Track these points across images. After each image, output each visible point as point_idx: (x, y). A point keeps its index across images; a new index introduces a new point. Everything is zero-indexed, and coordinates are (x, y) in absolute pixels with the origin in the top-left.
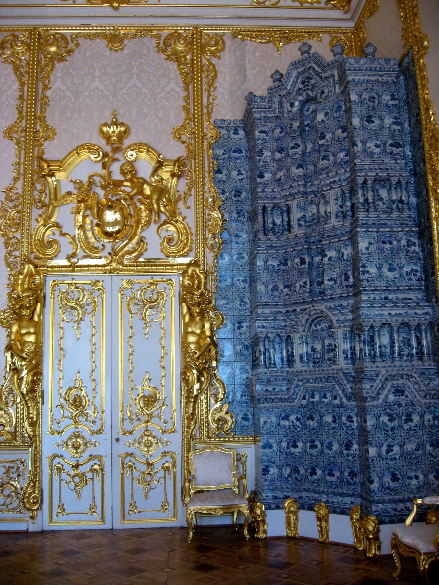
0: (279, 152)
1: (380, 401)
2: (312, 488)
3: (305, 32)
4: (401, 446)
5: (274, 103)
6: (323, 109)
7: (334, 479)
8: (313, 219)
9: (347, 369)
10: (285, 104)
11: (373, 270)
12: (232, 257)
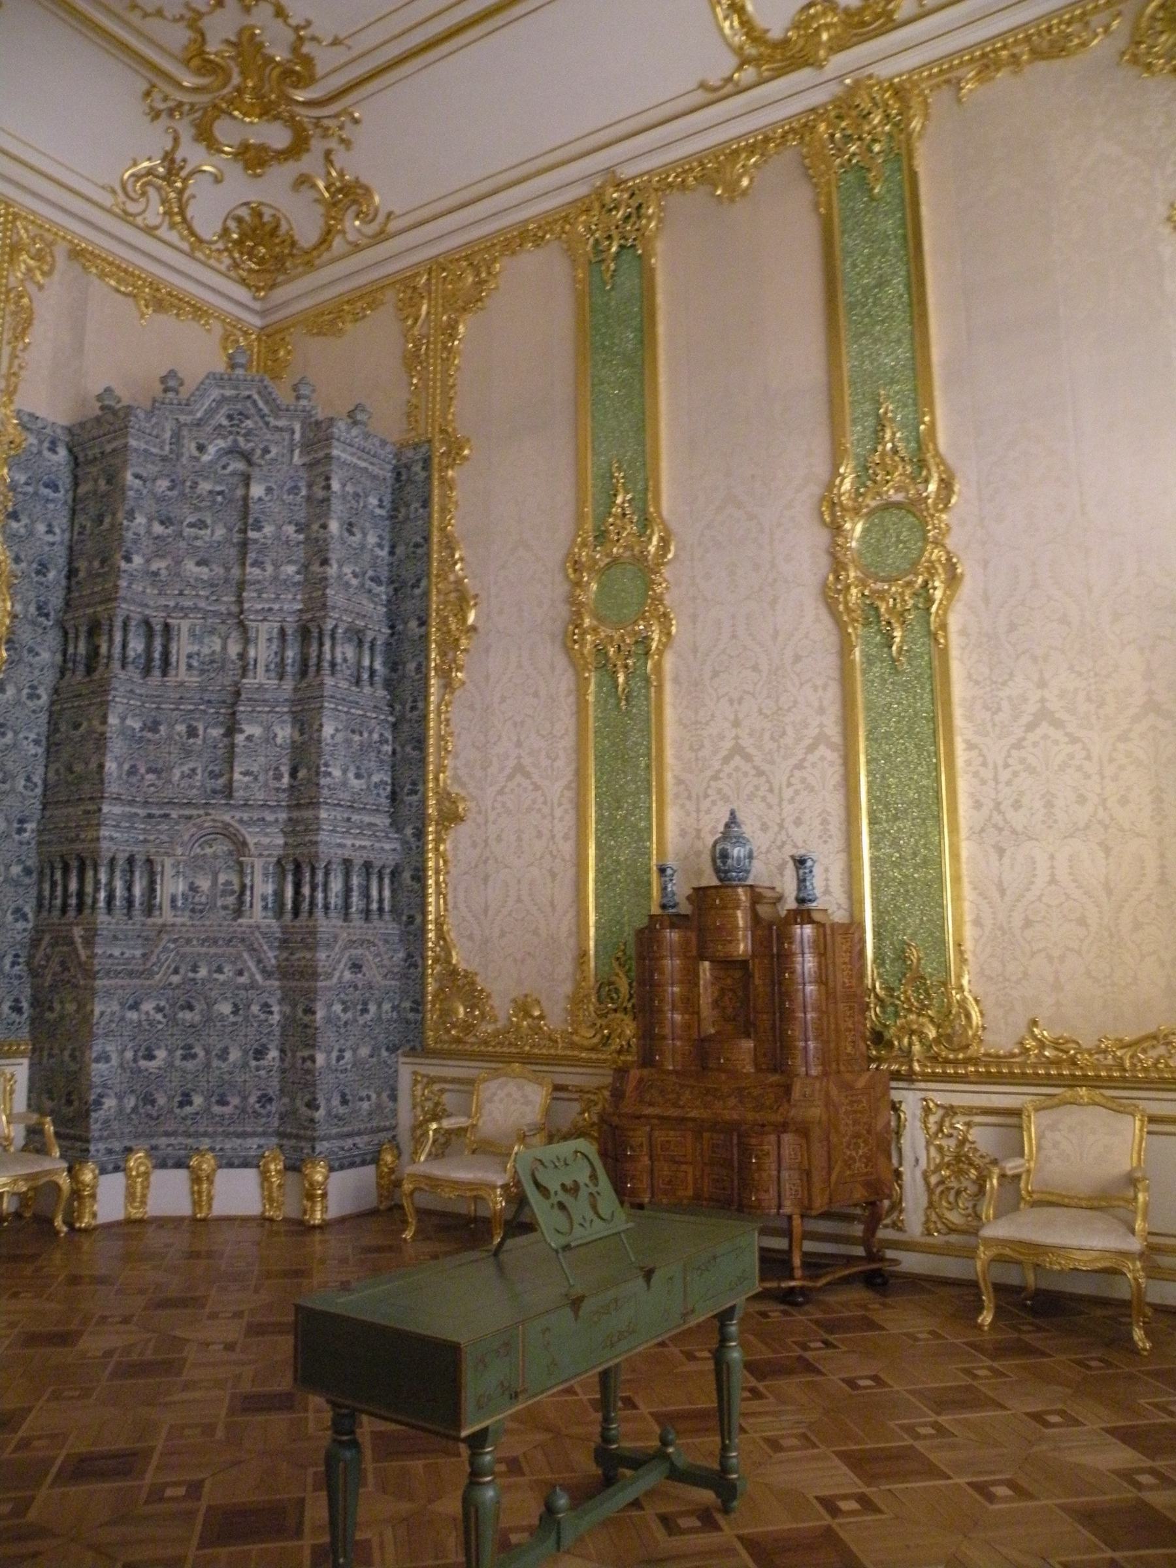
0: (162, 523)
1: (335, 980)
2: (182, 1128)
3: (188, 303)
4: (355, 1051)
5: (163, 430)
6: (265, 479)
7: (227, 1110)
8: (212, 662)
9: (269, 926)
10: (186, 441)
11: (337, 773)
12: (20, 691)
